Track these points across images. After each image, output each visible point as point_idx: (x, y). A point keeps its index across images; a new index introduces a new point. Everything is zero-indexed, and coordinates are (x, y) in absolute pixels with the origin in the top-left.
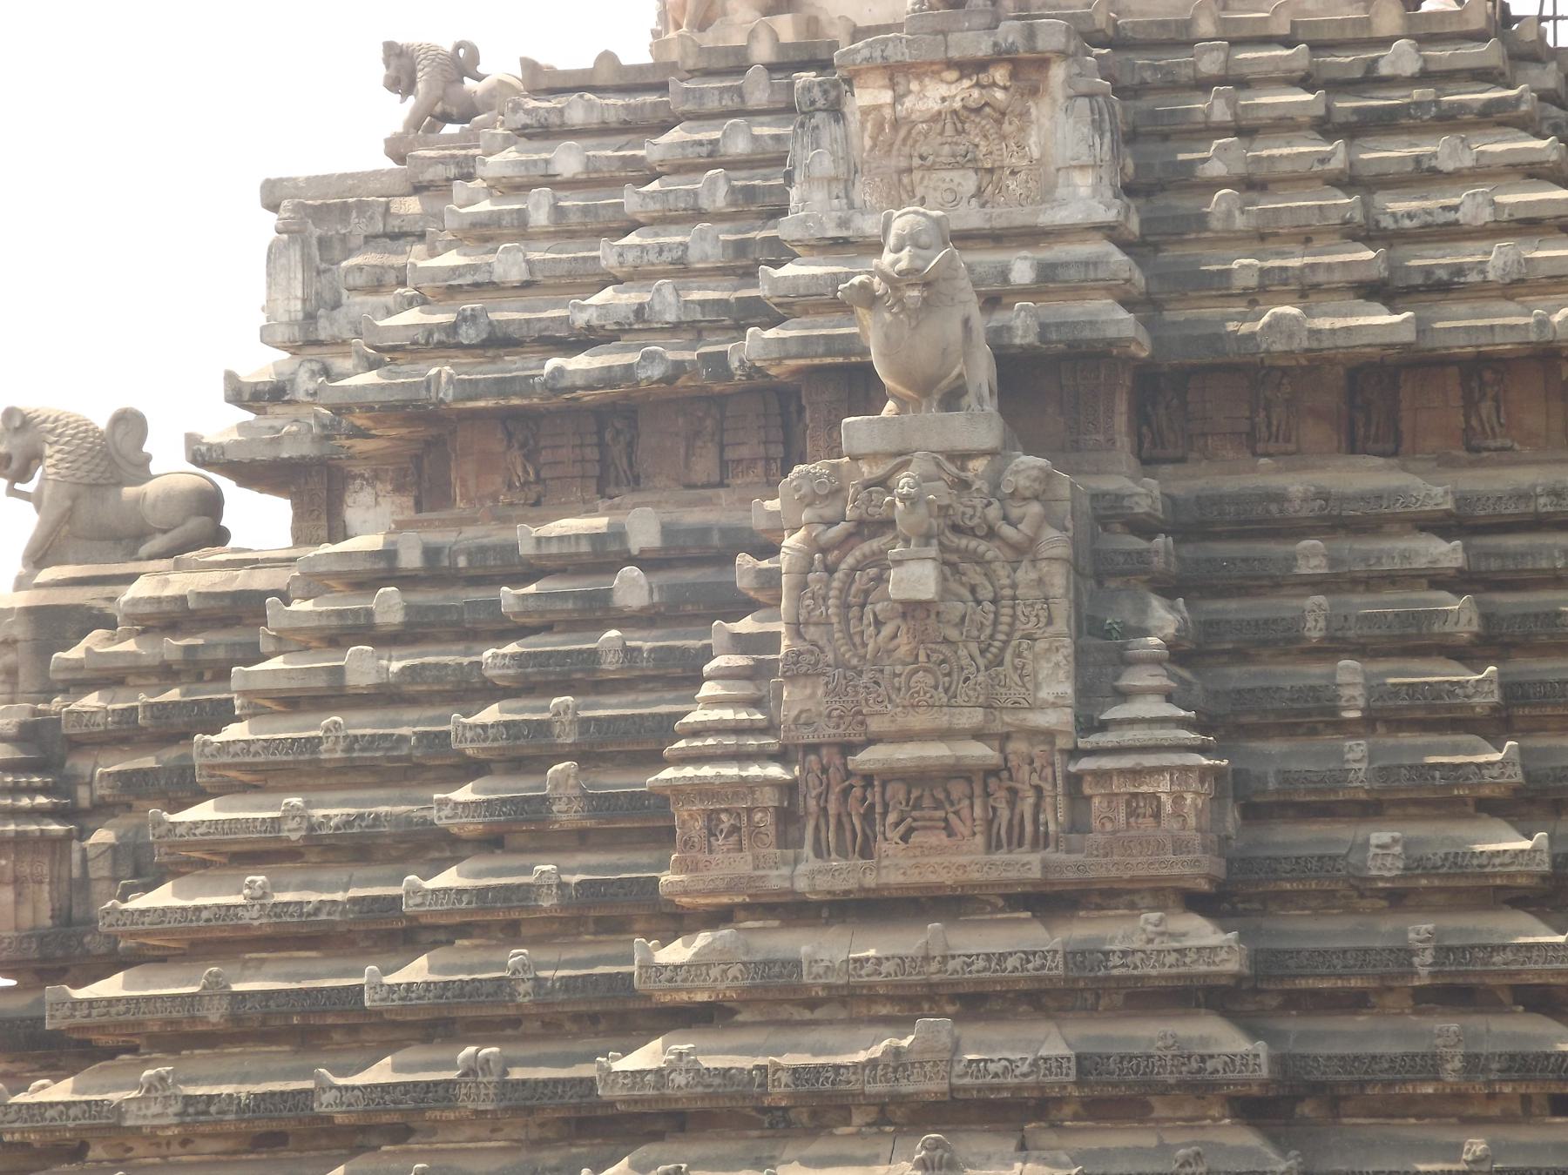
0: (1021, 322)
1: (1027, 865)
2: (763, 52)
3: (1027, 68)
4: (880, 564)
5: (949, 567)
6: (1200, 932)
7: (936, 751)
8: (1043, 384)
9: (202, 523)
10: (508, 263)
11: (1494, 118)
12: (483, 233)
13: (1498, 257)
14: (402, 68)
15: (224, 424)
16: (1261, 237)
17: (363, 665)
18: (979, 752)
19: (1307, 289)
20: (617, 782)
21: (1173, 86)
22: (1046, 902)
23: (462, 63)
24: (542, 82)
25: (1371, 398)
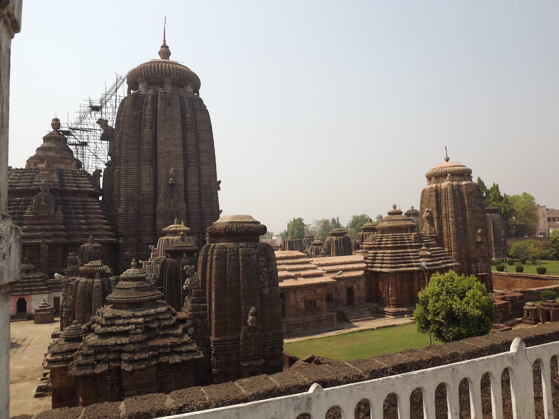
0: (52, 187)
1: (50, 222)
3: (53, 171)
5: (46, 203)
6: (62, 226)
10: (14, 181)
12: (12, 179)
13: (84, 185)
19: (71, 186)
25: (75, 193)
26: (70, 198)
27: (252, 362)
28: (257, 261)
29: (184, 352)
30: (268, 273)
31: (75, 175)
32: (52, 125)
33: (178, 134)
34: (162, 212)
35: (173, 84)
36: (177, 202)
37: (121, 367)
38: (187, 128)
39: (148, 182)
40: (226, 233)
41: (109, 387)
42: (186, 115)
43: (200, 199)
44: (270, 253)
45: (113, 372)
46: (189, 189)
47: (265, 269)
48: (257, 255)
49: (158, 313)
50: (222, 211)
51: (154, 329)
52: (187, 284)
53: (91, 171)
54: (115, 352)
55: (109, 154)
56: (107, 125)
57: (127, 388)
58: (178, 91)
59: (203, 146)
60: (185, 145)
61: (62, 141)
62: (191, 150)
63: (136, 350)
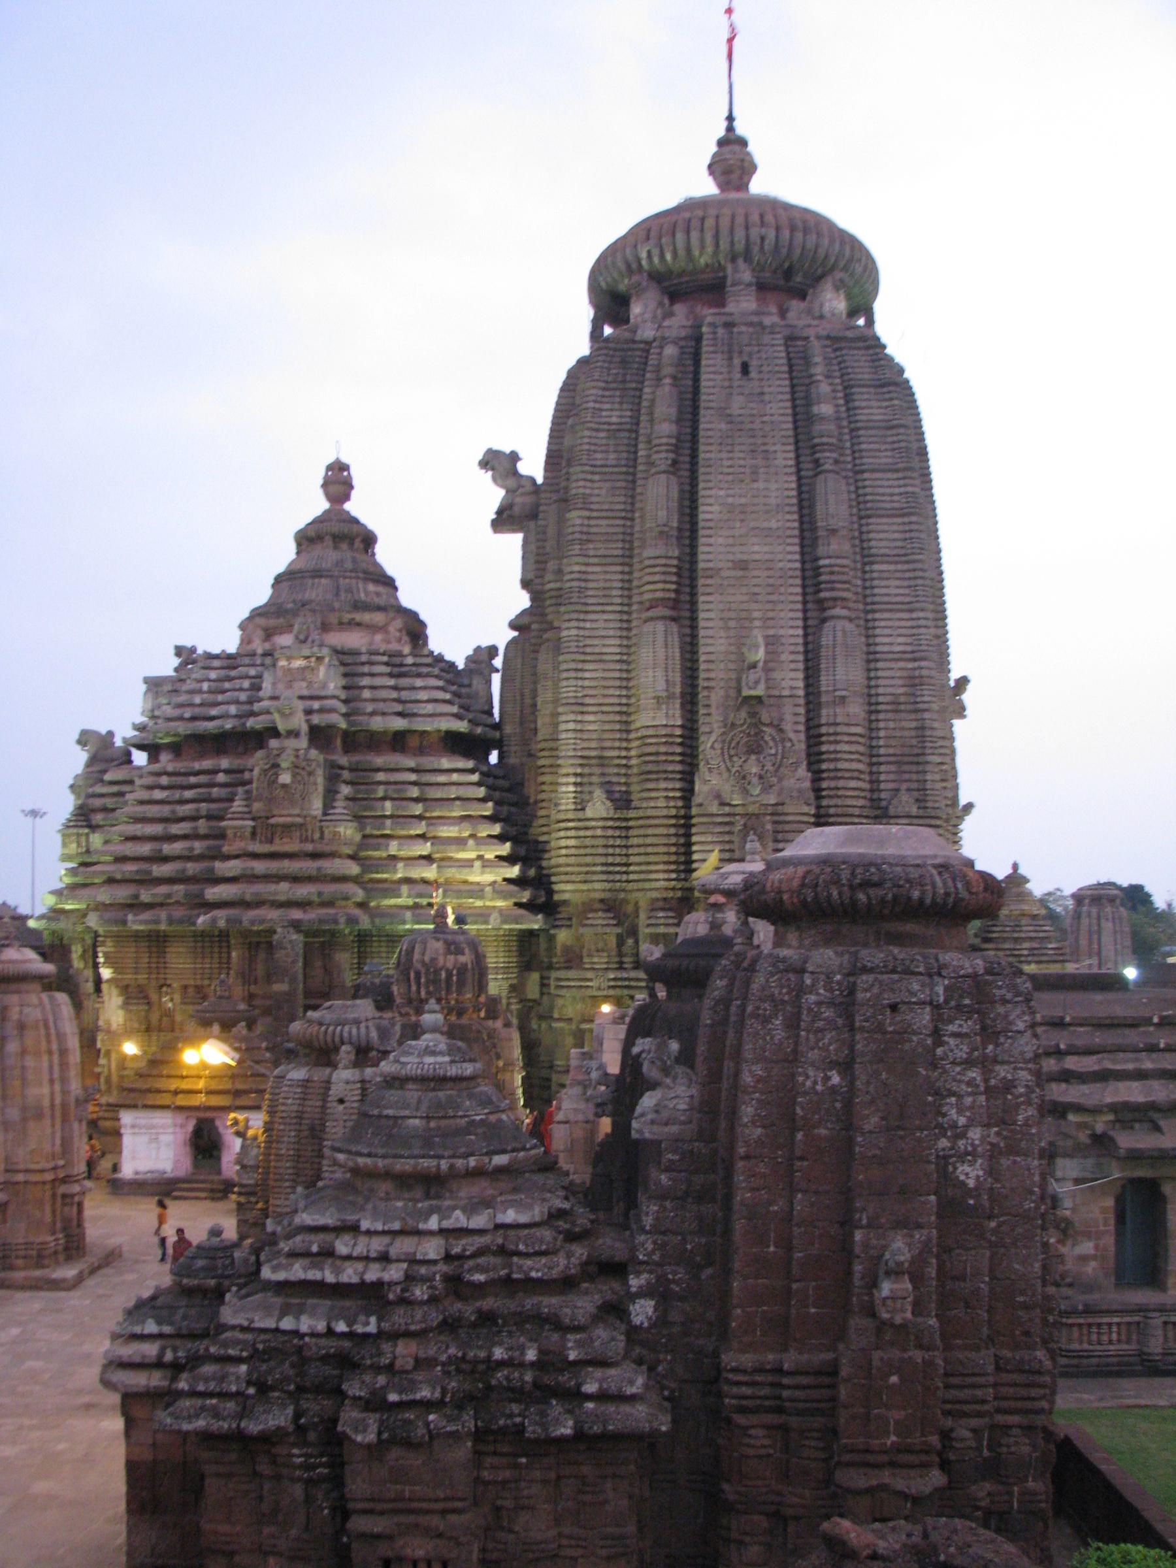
0: (316, 719)
1: (309, 847)
2: (260, 651)
3: (320, 659)
4: (277, 775)
5: (294, 776)
7: (289, 819)
8: (319, 736)
9: (126, 759)
11: (428, 675)
12: (192, 692)
14: (179, 651)
15: (131, 733)
16: (373, 700)
17: (158, 795)
18: (299, 820)
20: (213, 823)
21: (356, 664)
22: (315, 856)
23: (193, 650)
24: (209, 656)
25: (398, 741)
26: (379, 761)
27: (886, 1477)
28: (936, 1033)
29: (589, 1397)
30: (988, 1091)
31: (398, 669)
32: (326, 485)
33: (779, 487)
34: (714, 808)
35: (762, 287)
36: (776, 771)
37: (335, 1421)
38: (817, 462)
39: (661, 685)
40: (804, 903)
41: (298, 1490)
42: (815, 410)
43: (872, 753)
44: (1004, 1001)
45: (312, 1436)
46: (825, 714)
47: (974, 1074)
48: (936, 1007)
49: (498, 1226)
50: (969, 807)
51: (480, 1289)
52: (642, 1115)
53: (458, 656)
54: (325, 1359)
55: (526, 584)
56: (515, 473)
57: (360, 1506)
58: (783, 313)
59: (885, 535)
60: (808, 534)
61: (358, 543)
62: (836, 551)
63: (399, 1363)
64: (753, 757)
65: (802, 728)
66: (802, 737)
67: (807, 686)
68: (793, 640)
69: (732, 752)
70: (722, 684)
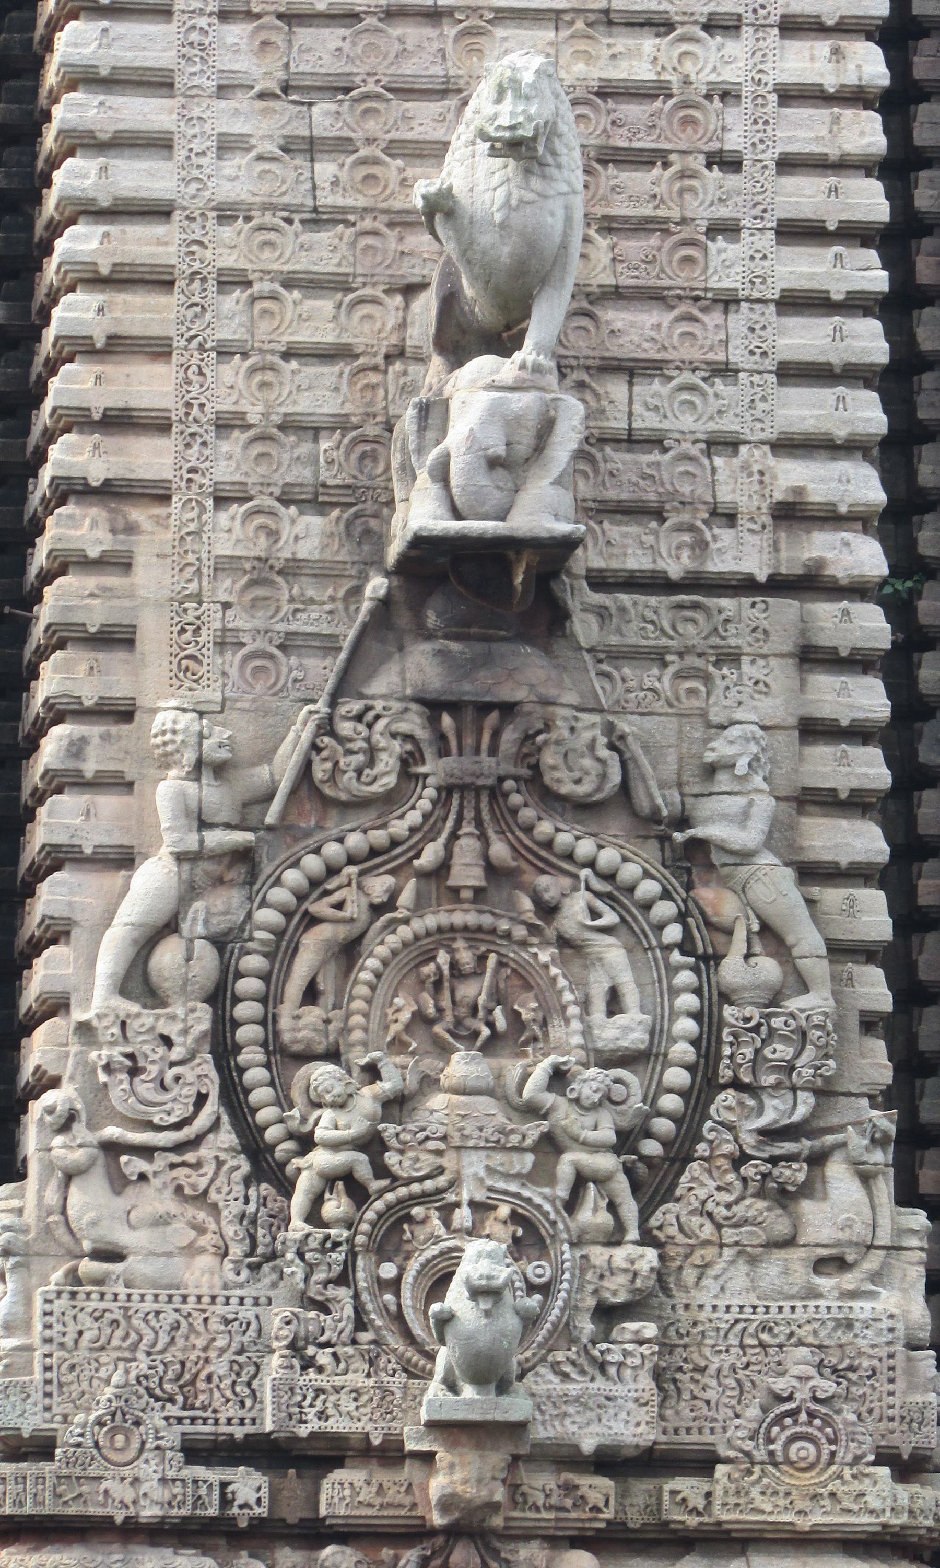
36: (654, 1184)
64: (462, 1065)
65: (867, 841)
66: (871, 915)
67: (894, 523)
68: (807, 130)
69: (300, 1024)
70: (228, 461)
